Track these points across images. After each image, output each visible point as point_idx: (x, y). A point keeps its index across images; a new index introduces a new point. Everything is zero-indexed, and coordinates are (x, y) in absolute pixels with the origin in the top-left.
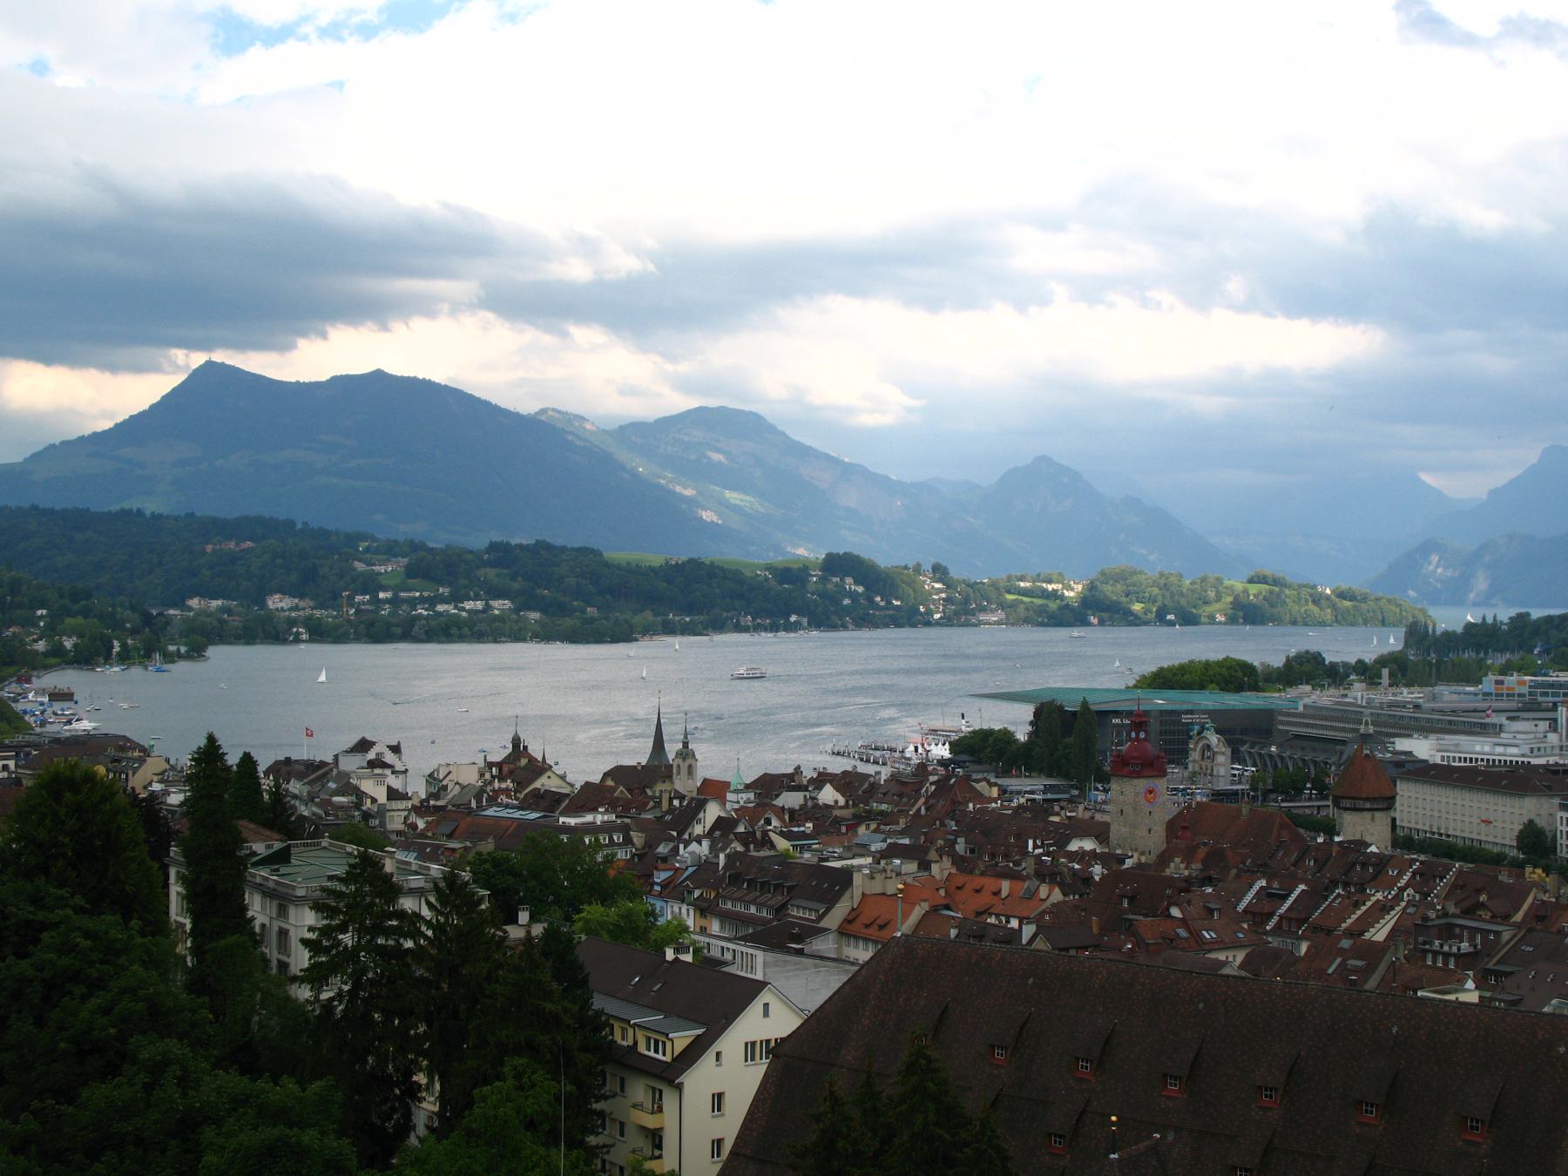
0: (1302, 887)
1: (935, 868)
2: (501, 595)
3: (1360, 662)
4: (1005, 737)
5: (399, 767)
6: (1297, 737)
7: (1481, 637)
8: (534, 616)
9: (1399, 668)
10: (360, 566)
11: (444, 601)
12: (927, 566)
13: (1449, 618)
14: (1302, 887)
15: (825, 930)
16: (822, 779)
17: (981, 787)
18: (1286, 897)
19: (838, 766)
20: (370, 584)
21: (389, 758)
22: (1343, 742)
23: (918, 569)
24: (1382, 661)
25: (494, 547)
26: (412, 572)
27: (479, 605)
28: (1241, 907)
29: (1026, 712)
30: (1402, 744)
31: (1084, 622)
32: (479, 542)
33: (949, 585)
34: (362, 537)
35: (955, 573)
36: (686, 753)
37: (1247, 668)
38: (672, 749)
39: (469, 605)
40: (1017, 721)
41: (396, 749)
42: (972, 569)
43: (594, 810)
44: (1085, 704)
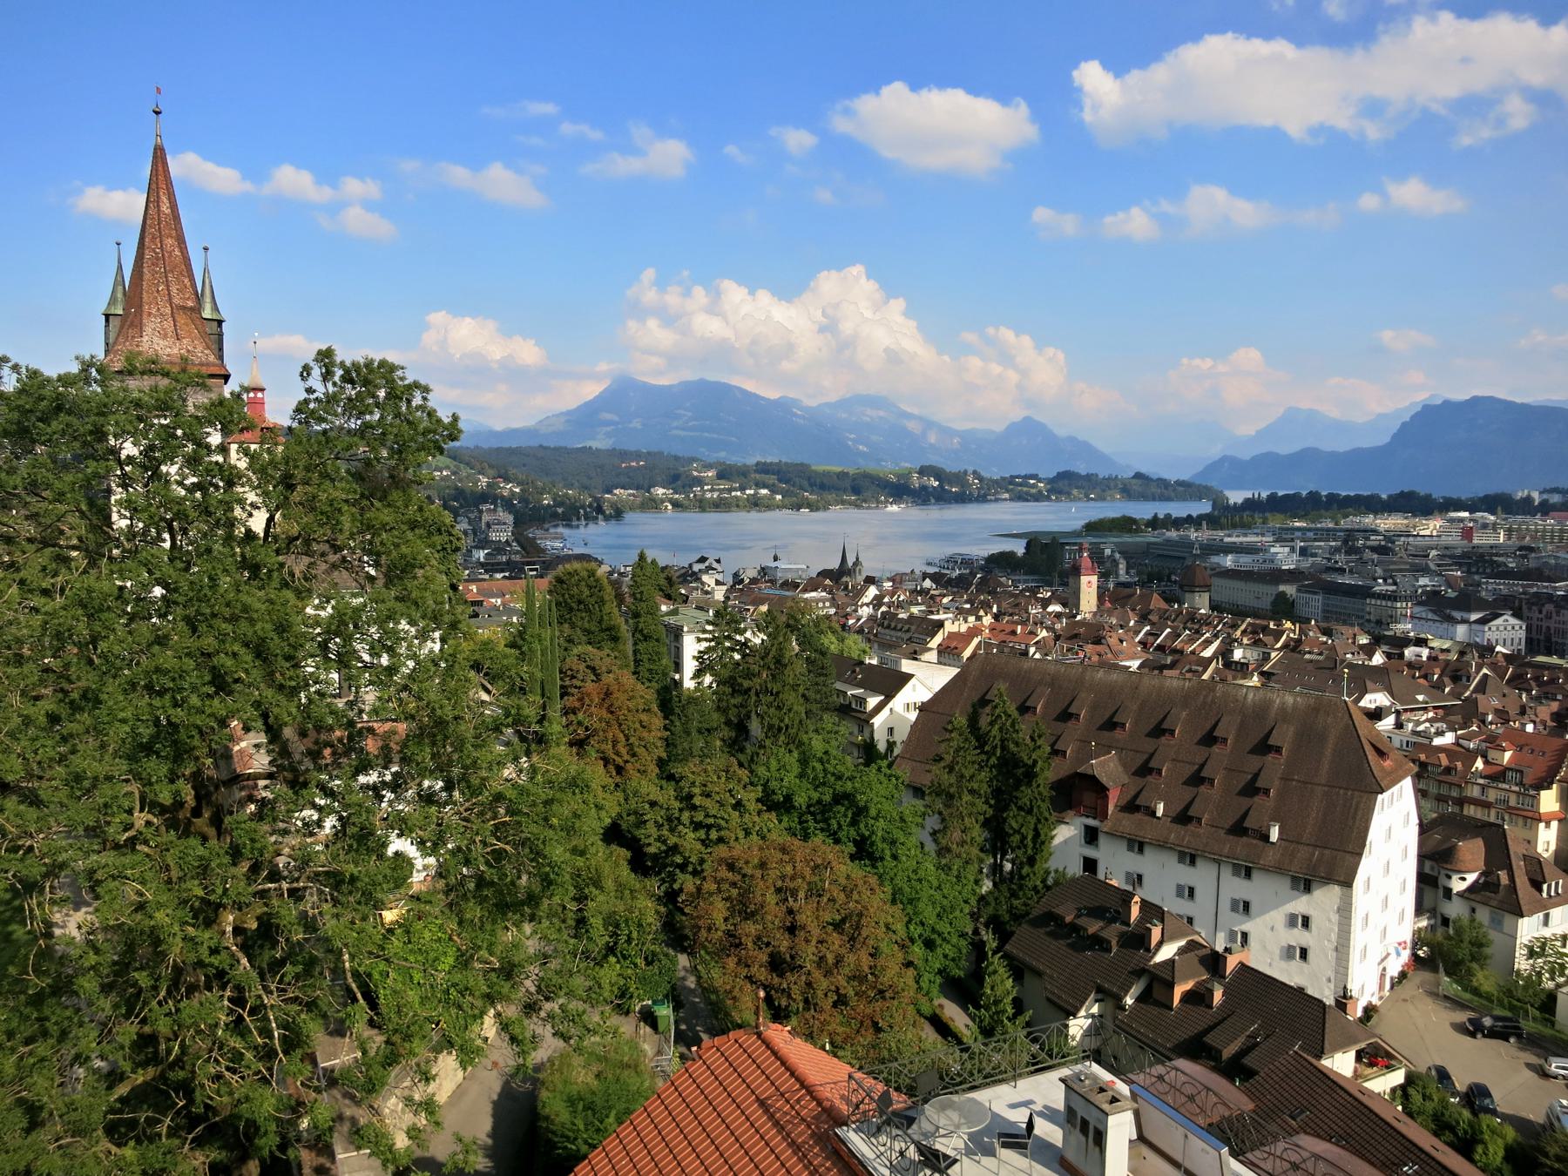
0: (1168, 630)
1: (984, 619)
2: (765, 487)
3: (1190, 516)
4: (1011, 554)
5: (720, 569)
6: (1159, 555)
7: (1250, 505)
8: (779, 497)
9: (1212, 521)
10: (695, 473)
11: (735, 490)
12: (970, 470)
13: (1236, 497)
14: (1168, 630)
15: (931, 649)
16: (925, 576)
17: (1003, 579)
18: (1159, 636)
19: (931, 570)
20: (700, 482)
21: (715, 565)
22: (1184, 558)
23: (965, 472)
24: (1201, 517)
25: (758, 464)
26: (720, 476)
27: (752, 492)
28: (1137, 640)
29: (1023, 542)
30: (1215, 559)
31: (1048, 498)
32: (751, 461)
33: (981, 479)
34: (694, 460)
35: (985, 474)
36: (857, 563)
37: (1132, 521)
38: (850, 562)
39: (748, 492)
40: (1019, 548)
41: (718, 561)
42: (994, 473)
43: (816, 590)
44: (1054, 539)
